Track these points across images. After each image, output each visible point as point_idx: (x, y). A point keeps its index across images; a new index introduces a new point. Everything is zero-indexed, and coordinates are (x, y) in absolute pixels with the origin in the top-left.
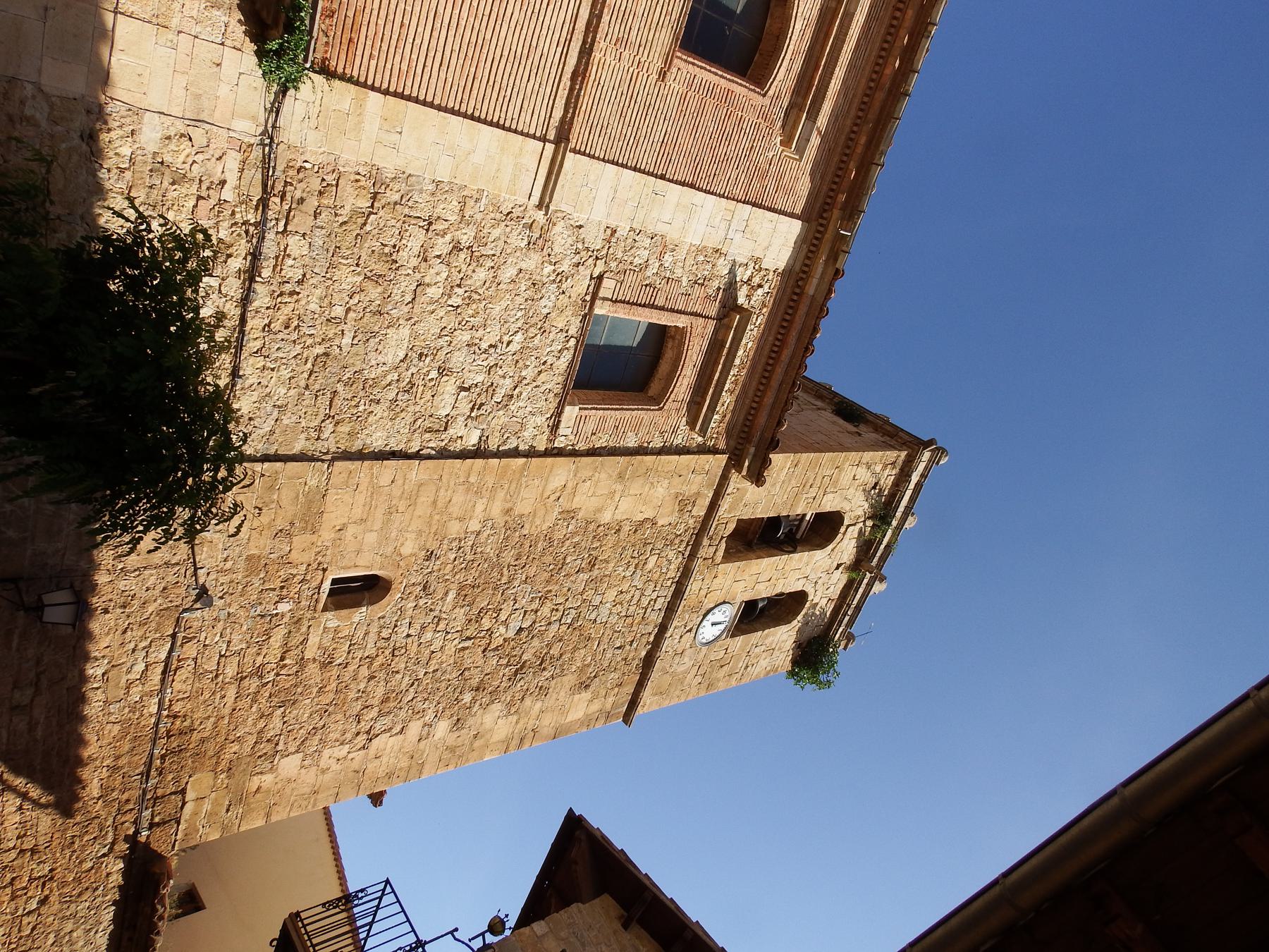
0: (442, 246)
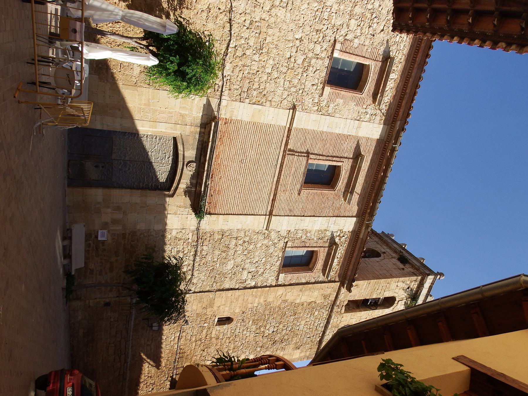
0: (241, 242)
